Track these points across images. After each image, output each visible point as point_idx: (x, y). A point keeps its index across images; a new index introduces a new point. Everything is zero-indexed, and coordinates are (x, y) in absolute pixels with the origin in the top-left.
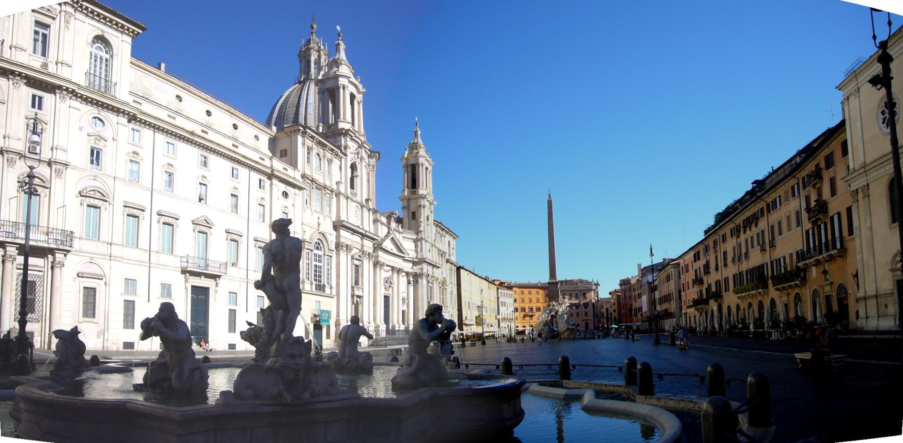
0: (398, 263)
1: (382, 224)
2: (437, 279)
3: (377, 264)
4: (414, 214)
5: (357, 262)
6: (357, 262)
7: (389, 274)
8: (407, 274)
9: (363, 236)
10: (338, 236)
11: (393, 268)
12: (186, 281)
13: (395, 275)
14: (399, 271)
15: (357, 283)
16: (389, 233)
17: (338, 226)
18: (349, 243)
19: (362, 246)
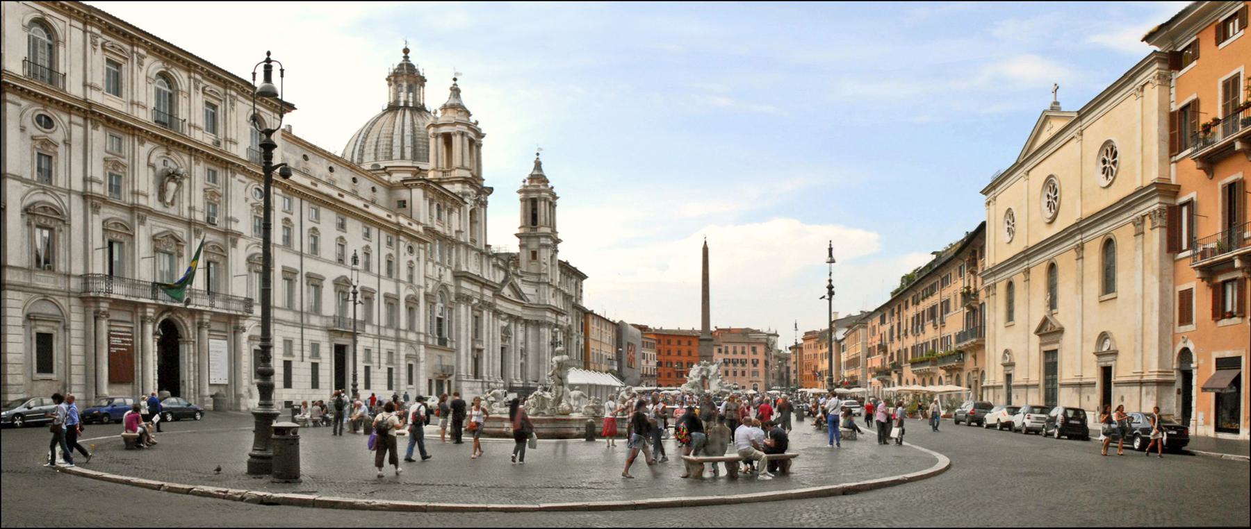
0: (517, 310)
1: (500, 268)
2: (561, 328)
3: (497, 313)
4: (534, 254)
5: (477, 313)
6: (477, 313)
7: (505, 324)
8: (527, 322)
9: (484, 284)
10: (458, 287)
11: (510, 316)
12: (331, 341)
13: (513, 325)
14: (517, 319)
15: (476, 336)
16: (506, 277)
17: (459, 276)
18: (469, 293)
19: (482, 295)
